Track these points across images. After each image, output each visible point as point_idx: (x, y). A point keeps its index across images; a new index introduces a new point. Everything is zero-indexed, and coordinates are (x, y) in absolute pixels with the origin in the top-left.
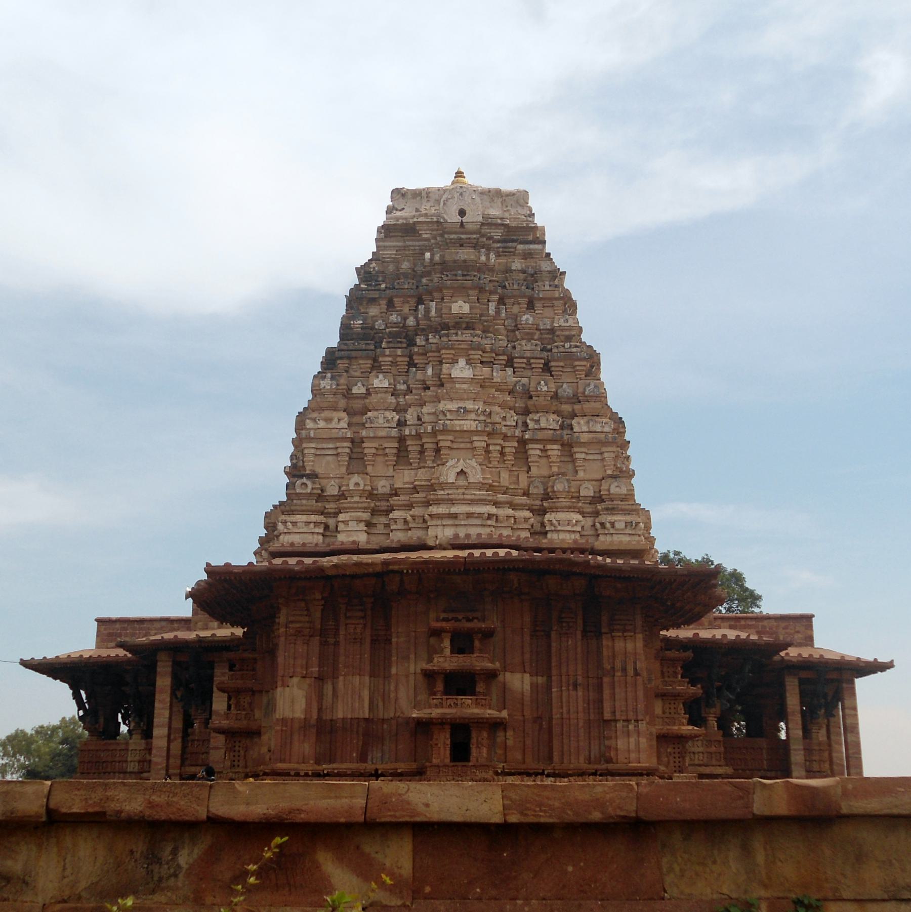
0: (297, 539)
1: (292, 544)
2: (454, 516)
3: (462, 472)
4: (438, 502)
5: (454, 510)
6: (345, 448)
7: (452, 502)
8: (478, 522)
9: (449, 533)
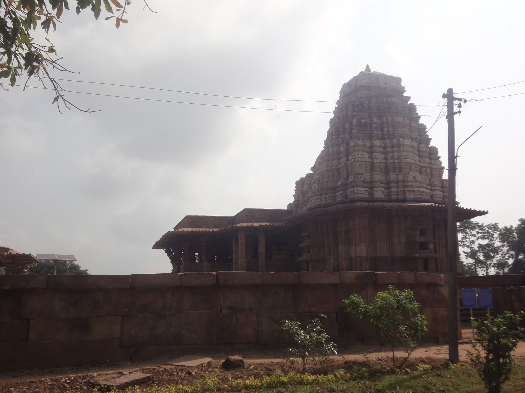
0: (360, 196)
1: (361, 198)
2: (414, 191)
3: (414, 177)
4: (409, 186)
5: (414, 189)
6: (369, 165)
7: (413, 187)
8: (420, 194)
9: (412, 196)
